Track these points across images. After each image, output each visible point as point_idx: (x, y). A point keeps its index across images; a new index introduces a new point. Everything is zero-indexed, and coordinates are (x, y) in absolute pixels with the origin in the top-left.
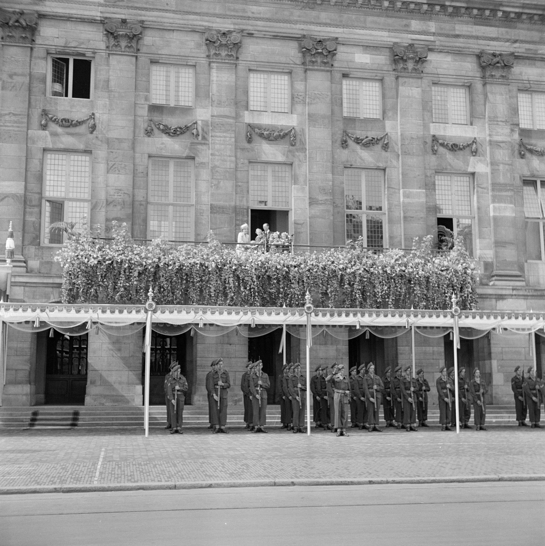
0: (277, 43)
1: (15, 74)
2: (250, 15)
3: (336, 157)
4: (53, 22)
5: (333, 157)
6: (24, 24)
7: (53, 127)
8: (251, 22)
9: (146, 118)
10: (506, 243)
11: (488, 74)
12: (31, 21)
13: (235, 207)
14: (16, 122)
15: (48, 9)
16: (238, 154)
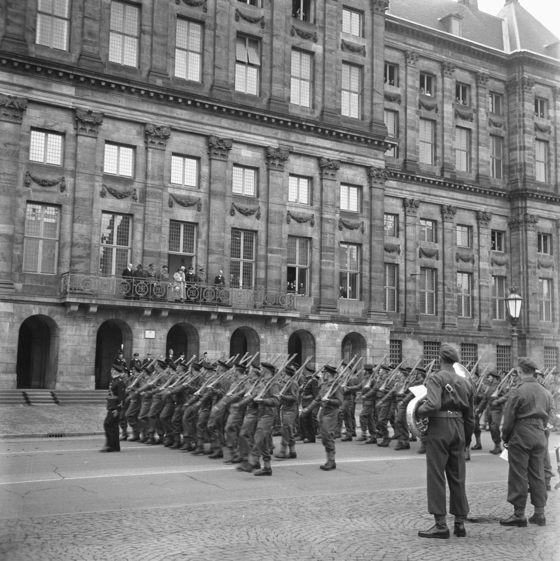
0: (192, 137)
1: (9, 144)
2: (175, 115)
3: (227, 221)
4: (36, 106)
5: (225, 222)
6: (17, 106)
7: (34, 186)
8: (176, 121)
9: (101, 183)
10: (328, 286)
11: (324, 172)
12: (22, 105)
13: (160, 252)
14: (9, 180)
15: (34, 97)
16: (164, 214)
